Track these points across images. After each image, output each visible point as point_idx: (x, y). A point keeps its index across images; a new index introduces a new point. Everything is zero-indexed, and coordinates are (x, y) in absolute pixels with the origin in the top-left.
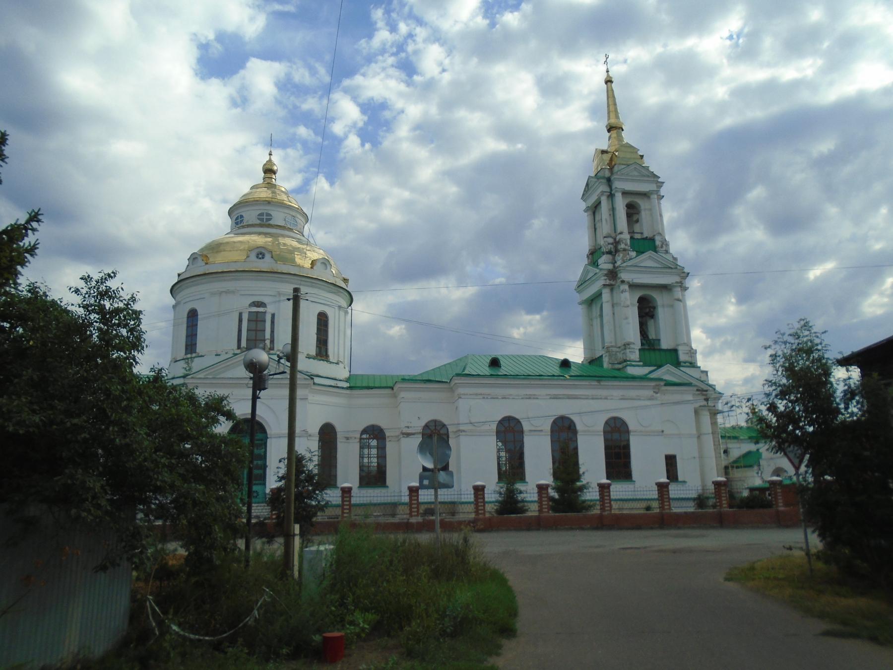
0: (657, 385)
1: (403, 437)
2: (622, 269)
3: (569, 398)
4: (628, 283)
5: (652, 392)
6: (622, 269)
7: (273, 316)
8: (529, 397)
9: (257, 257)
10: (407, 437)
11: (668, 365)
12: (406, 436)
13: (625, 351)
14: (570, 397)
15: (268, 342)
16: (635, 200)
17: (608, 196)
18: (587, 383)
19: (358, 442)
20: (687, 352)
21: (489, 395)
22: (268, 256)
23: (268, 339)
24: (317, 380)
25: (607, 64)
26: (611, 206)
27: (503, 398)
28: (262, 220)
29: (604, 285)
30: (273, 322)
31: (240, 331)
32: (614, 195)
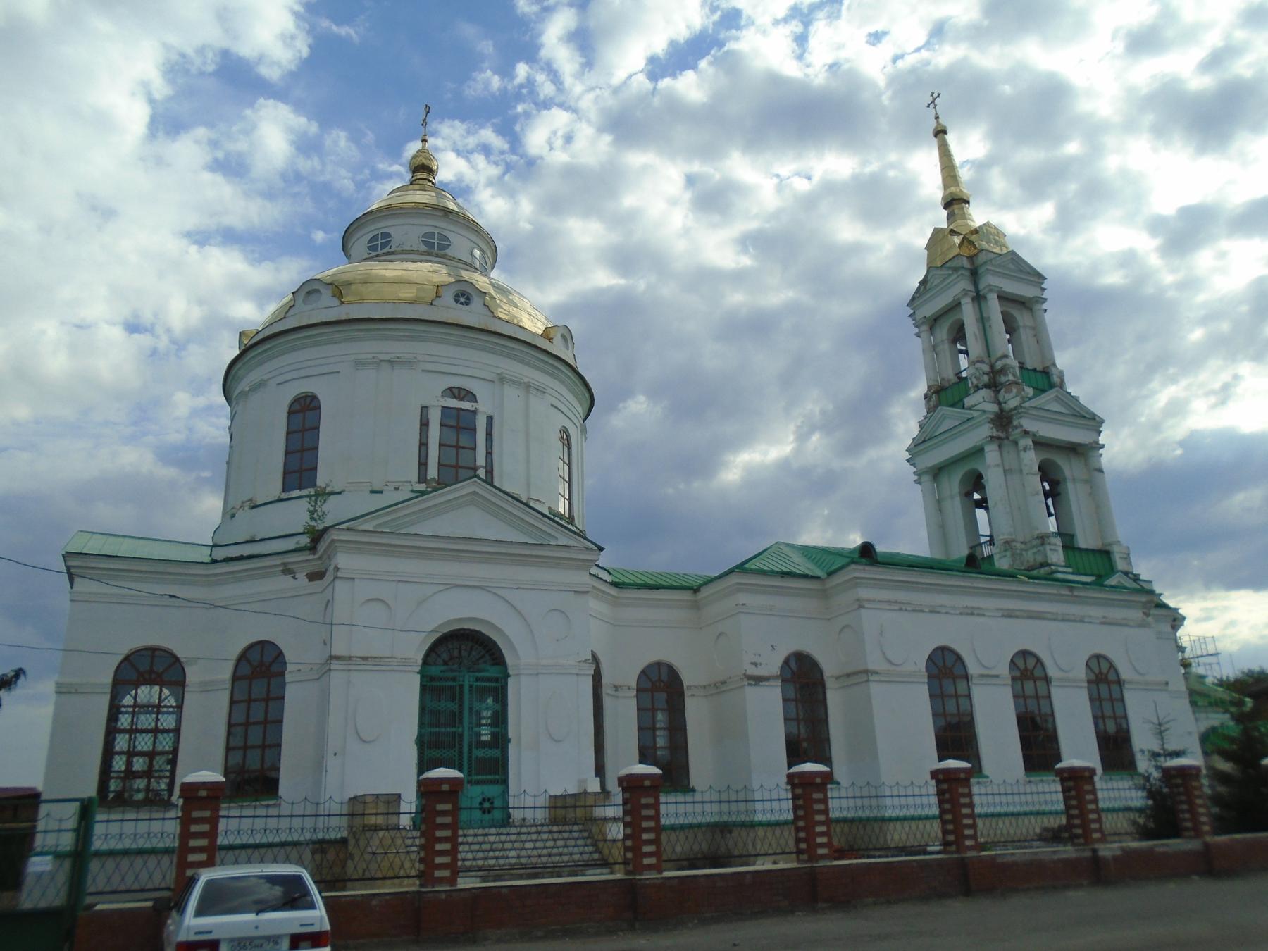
1: (750, 685)
2: (1025, 413)
4: (1034, 435)
5: (1142, 614)
6: (1025, 413)
7: (490, 420)
8: (972, 612)
9: (457, 301)
10: (755, 685)
12: (753, 683)
13: (1041, 548)
16: (1009, 310)
17: (973, 299)
18: (1055, 592)
19: (634, 697)
22: (476, 303)
23: (483, 467)
25: (935, 108)
26: (979, 315)
27: (931, 612)
28: (431, 245)
29: (992, 437)
30: (489, 434)
31: (423, 445)
32: (985, 298)
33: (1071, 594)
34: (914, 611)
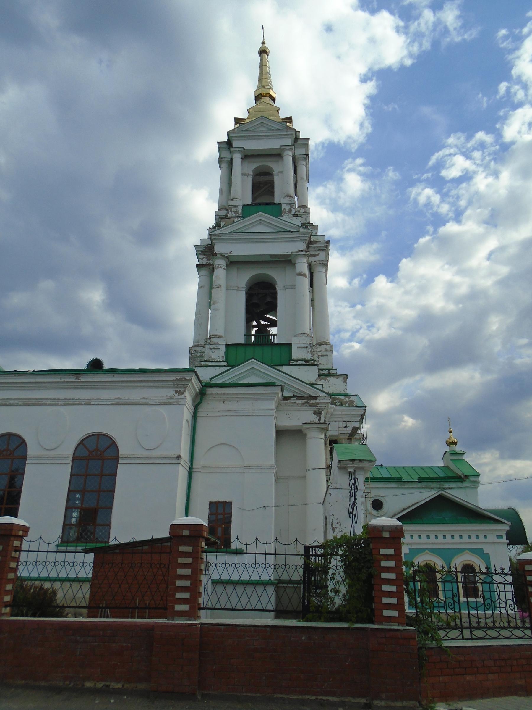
3: (25, 405)
5: (174, 392)
11: (253, 360)
14: (27, 403)
20: (305, 345)
33: (77, 380)
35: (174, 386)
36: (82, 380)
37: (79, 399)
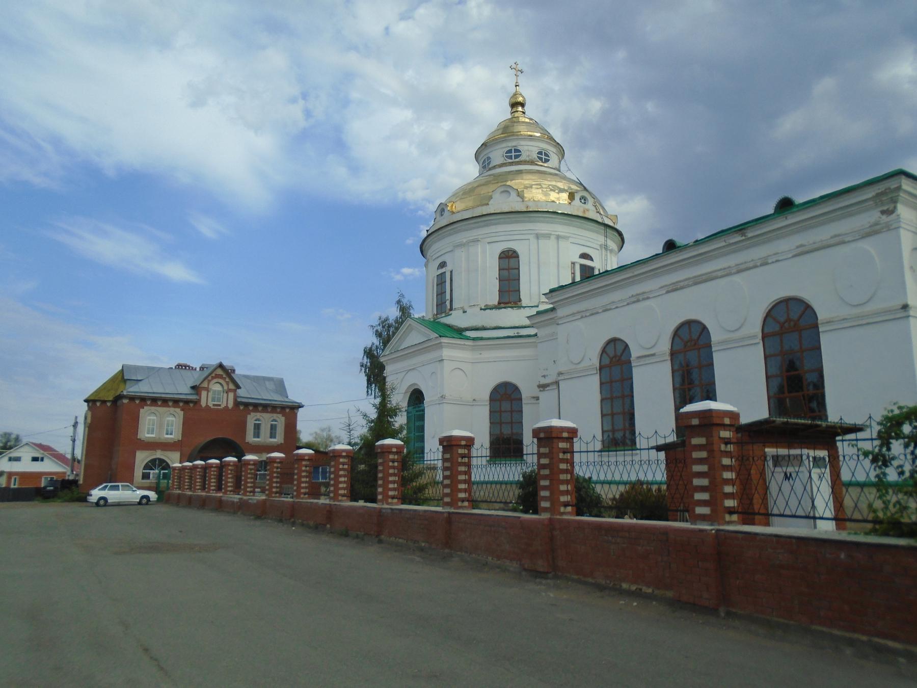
0: (878, 195)
3: (696, 284)
5: (879, 214)
7: (451, 272)
8: (637, 299)
12: (542, 389)
14: (698, 281)
15: (448, 303)
18: (723, 244)
21: (586, 311)
23: (448, 300)
24: (468, 334)
27: (604, 311)
33: (744, 238)
34: (592, 314)
35: (876, 205)
36: (750, 235)
37: (752, 260)
